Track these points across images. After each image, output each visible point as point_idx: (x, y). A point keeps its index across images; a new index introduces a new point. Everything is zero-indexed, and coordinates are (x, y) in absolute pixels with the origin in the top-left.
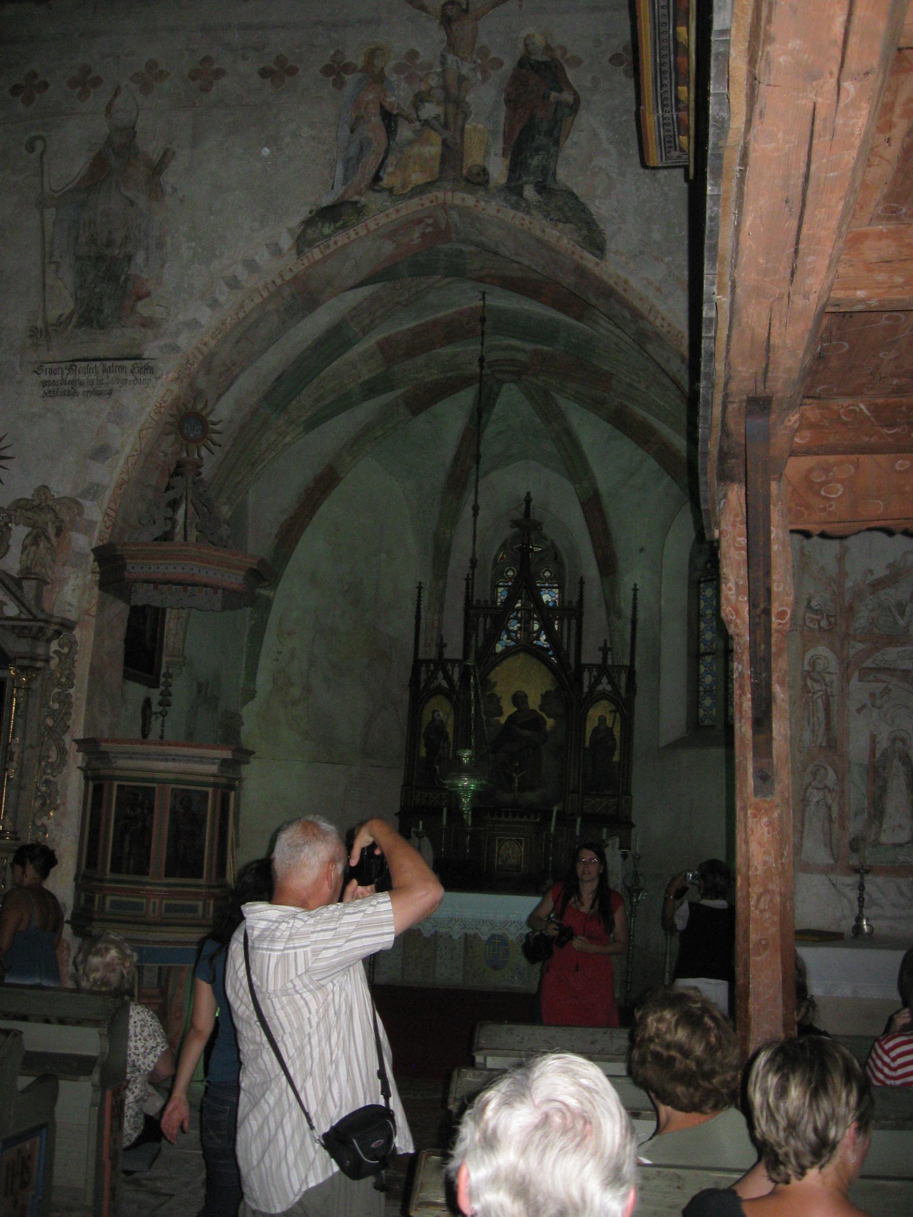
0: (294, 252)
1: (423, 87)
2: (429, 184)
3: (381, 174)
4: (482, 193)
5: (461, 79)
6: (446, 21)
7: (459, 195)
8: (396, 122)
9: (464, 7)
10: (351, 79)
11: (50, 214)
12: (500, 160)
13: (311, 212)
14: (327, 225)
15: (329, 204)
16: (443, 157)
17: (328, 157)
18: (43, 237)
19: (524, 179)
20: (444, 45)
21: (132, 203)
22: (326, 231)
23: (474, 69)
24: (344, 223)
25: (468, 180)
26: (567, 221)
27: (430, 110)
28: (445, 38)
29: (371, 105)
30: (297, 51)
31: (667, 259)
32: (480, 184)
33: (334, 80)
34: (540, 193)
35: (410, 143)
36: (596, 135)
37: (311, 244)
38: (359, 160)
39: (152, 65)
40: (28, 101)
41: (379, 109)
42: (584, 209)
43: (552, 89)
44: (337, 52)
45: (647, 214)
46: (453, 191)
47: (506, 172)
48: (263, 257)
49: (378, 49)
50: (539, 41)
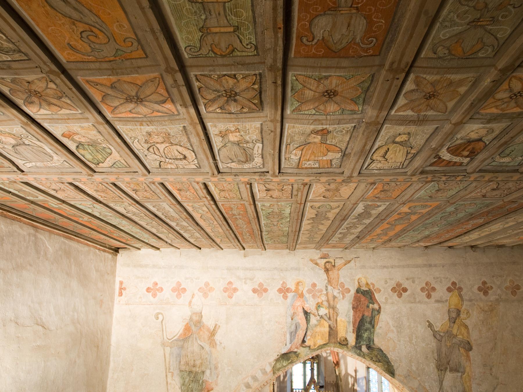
0: (272, 372)
1: (320, 301)
2: (325, 344)
3: (305, 339)
4: (346, 349)
5: (335, 297)
6: (327, 270)
8: (309, 316)
9: (333, 264)
10: (290, 295)
11: (168, 349)
13: (278, 356)
14: (285, 362)
15: (285, 352)
16: (329, 332)
17: (283, 330)
18: (165, 360)
19: (362, 343)
20: (326, 281)
21: (203, 348)
22: (285, 364)
23: (339, 293)
24: (292, 361)
25: (340, 343)
26: (380, 362)
27: (323, 311)
28: (327, 278)
29: (299, 308)
30: (267, 281)
31: (419, 378)
32: (345, 345)
33: (283, 295)
34: (368, 349)
35: (316, 326)
36: (388, 323)
37: (279, 370)
38: (296, 332)
39: (207, 284)
40: (154, 295)
41: (302, 311)
42: (386, 356)
43: (370, 303)
45: (410, 359)
46: (334, 347)
47: (355, 340)
48: (259, 375)
49: (300, 282)
50: (364, 281)
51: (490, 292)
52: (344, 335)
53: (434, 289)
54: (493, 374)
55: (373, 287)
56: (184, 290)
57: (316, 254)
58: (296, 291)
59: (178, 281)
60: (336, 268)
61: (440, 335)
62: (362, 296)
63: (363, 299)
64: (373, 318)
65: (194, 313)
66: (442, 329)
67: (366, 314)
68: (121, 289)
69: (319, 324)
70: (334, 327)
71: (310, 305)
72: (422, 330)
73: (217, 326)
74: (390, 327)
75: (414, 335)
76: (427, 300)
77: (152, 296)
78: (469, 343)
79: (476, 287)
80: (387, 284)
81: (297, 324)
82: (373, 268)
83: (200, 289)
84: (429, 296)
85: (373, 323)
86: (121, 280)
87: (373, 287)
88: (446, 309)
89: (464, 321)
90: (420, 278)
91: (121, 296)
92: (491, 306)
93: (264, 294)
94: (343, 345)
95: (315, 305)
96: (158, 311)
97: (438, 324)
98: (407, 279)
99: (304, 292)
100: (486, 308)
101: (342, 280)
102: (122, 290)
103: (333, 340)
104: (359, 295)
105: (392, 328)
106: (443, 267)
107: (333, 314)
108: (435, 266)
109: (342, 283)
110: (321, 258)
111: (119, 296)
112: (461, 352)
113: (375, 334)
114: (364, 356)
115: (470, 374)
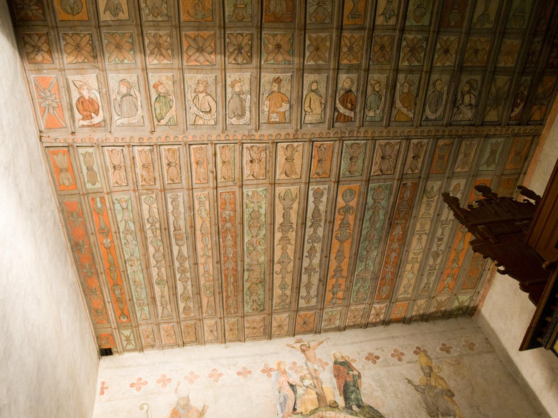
1: (302, 374)
2: (316, 409)
3: (296, 407)
4: (338, 410)
5: (316, 370)
6: (303, 351)
7: (328, 412)
8: (296, 388)
9: (308, 346)
10: (273, 374)
12: (340, 397)
16: (318, 398)
17: (273, 403)
19: (351, 403)
20: (305, 359)
23: (319, 366)
25: (330, 406)
27: (307, 382)
29: (284, 382)
32: (335, 407)
33: (267, 375)
34: (359, 408)
35: (303, 395)
36: (371, 385)
38: (285, 403)
39: (192, 373)
40: (139, 389)
41: (288, 384)
42: (377, 412)
43: (349, 370)
44: (266, 364)
46: (326, 411)
49: (281, 362)
51: (451, 350)
52: (332, 399)
53: (402, 354)
54: (482, 412)
55: (349, 359)
56: (170, 380)
57: (291, 340)
58: (279, 369)
59: (163, 374)
60: (311, 348)
61: (421, 388)
62: (340, 366)
63: (342, 368)
64: (355, 382)
65: (181, 399)
66: (422, 383)
67: (348, 379)
68: (102, 389)
69: (306, 393)
70: (321, 393)
71: (295, 379)
72: (403, 386)
73: (206, 407)
74: (373, 388)
75: (397, 391)
76: (400, 363)
77: (136, 390)
78: (449, 391)
79: (438, 348)
80: (361, 356)
81: (285, 396)
82: (344, 345)
83: (185, 378)
84: (400, 360)
85: (356, 386)
86: (103, 380)
87: (349, 359)
88: (418, 367)
89: (438, 374)
90: (387, 347)
91: (103, 394)
92: (456, 360)
93: (249, 375)
94: (334, 407)
95: (299, 379)
96: (143, 402)
97: (416, 380)
98: (377, 349)
99: (287, 369)
100: (453, 363)
101: (318, 356)
102: (104, 390)
103: (323, 405)
104: (337, 365)
105: (375, 388)
106: (404, 337)
107: (318, 383)
108: (398, 337)
109: (319, 359)
110: (296, 343)
111: (101, 394)
112: (446, 399)
113: (361, 395)
114: (356, 414)
115: (461, 415)
